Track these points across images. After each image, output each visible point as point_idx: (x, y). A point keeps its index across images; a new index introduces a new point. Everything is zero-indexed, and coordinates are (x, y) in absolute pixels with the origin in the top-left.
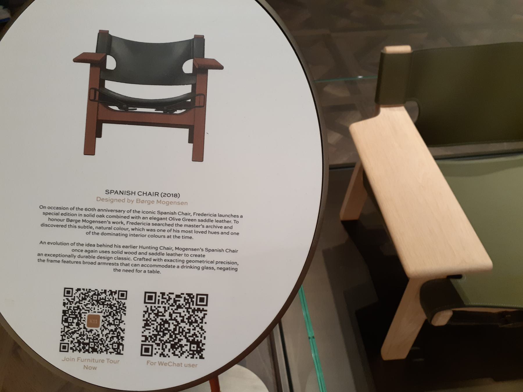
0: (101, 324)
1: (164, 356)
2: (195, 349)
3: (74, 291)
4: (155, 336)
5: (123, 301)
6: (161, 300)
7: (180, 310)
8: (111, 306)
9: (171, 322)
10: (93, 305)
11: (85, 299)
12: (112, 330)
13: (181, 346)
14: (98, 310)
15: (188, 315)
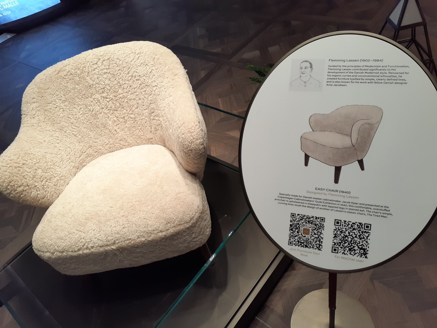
0: (310, 233)
1: (345, 254)
2: (363, 252)
3: (296, 215)
4: (340, 243)
5: (323, 223)
6: (344, 225)
7: (354, 231)
8: (316, 225)
9: (349, 237)
10: (306, 223)
11: (302, 220)
12: (316, 237)
13: (355, 250)
14: (308, 226)
15: (359, 234)
